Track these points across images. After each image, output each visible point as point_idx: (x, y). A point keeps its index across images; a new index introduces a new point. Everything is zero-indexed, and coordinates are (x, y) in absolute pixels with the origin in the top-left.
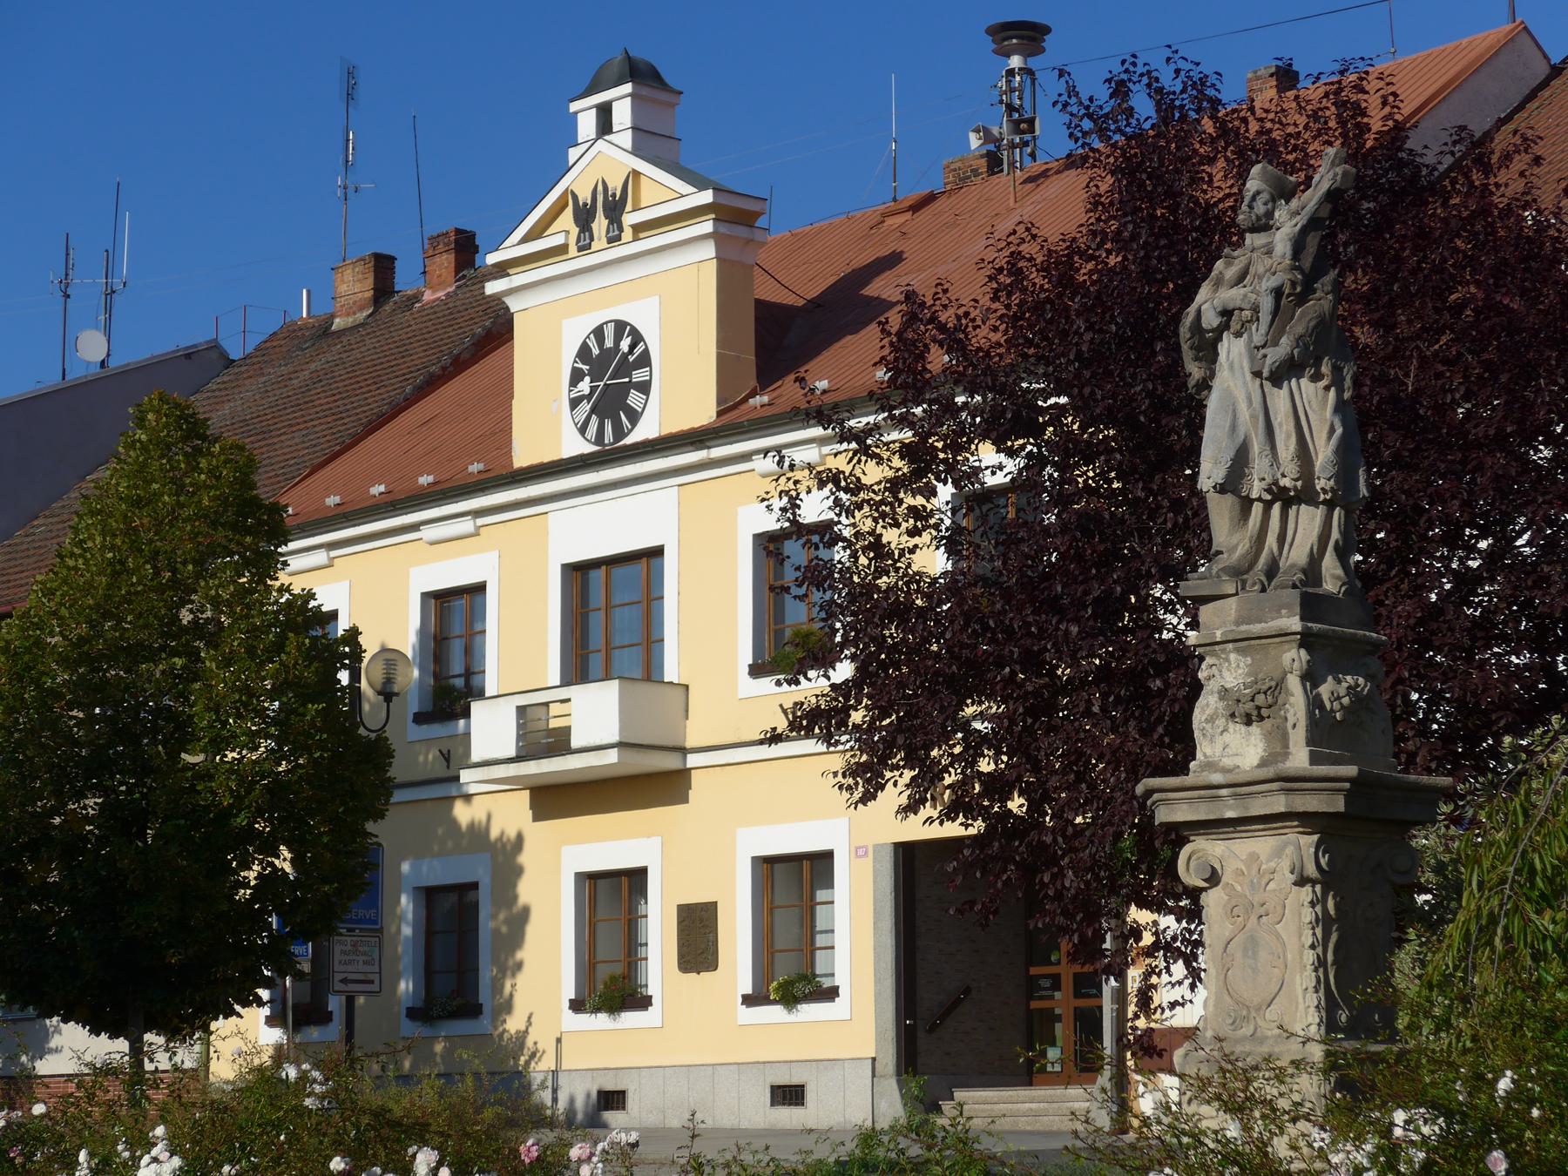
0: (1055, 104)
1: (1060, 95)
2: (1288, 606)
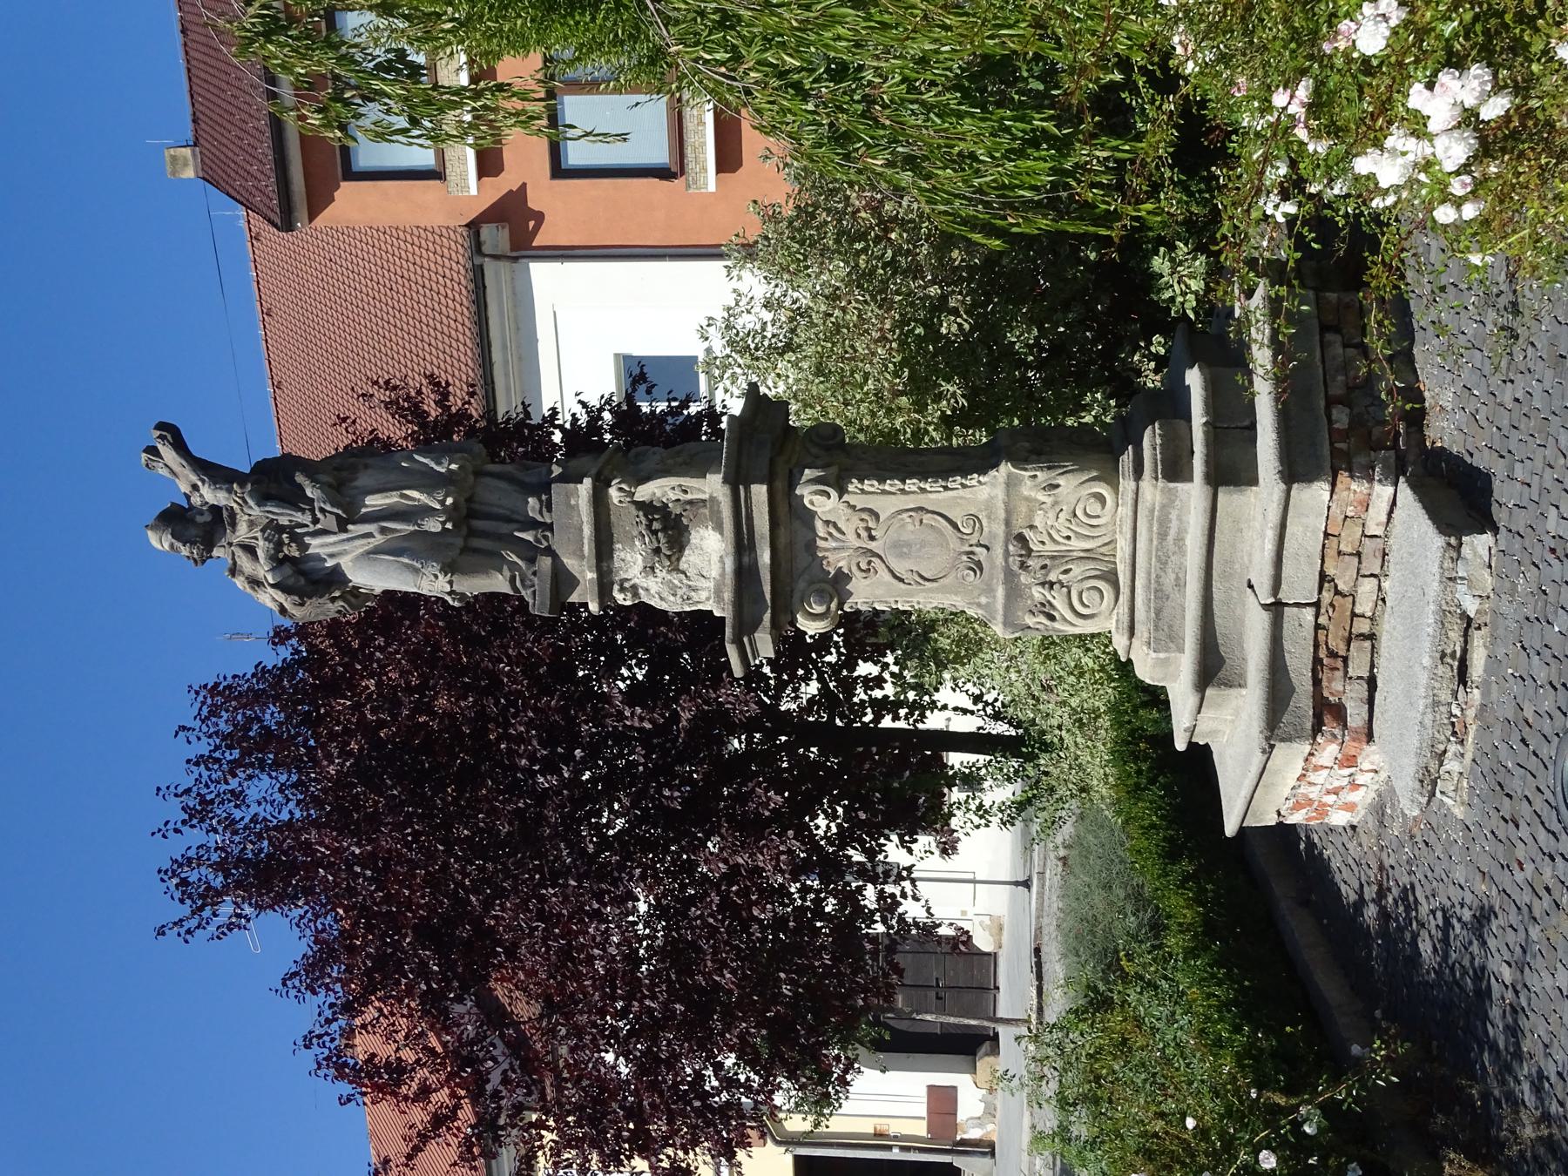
0: (186, 942)
1: (179, 935)
2: (568, 496)
